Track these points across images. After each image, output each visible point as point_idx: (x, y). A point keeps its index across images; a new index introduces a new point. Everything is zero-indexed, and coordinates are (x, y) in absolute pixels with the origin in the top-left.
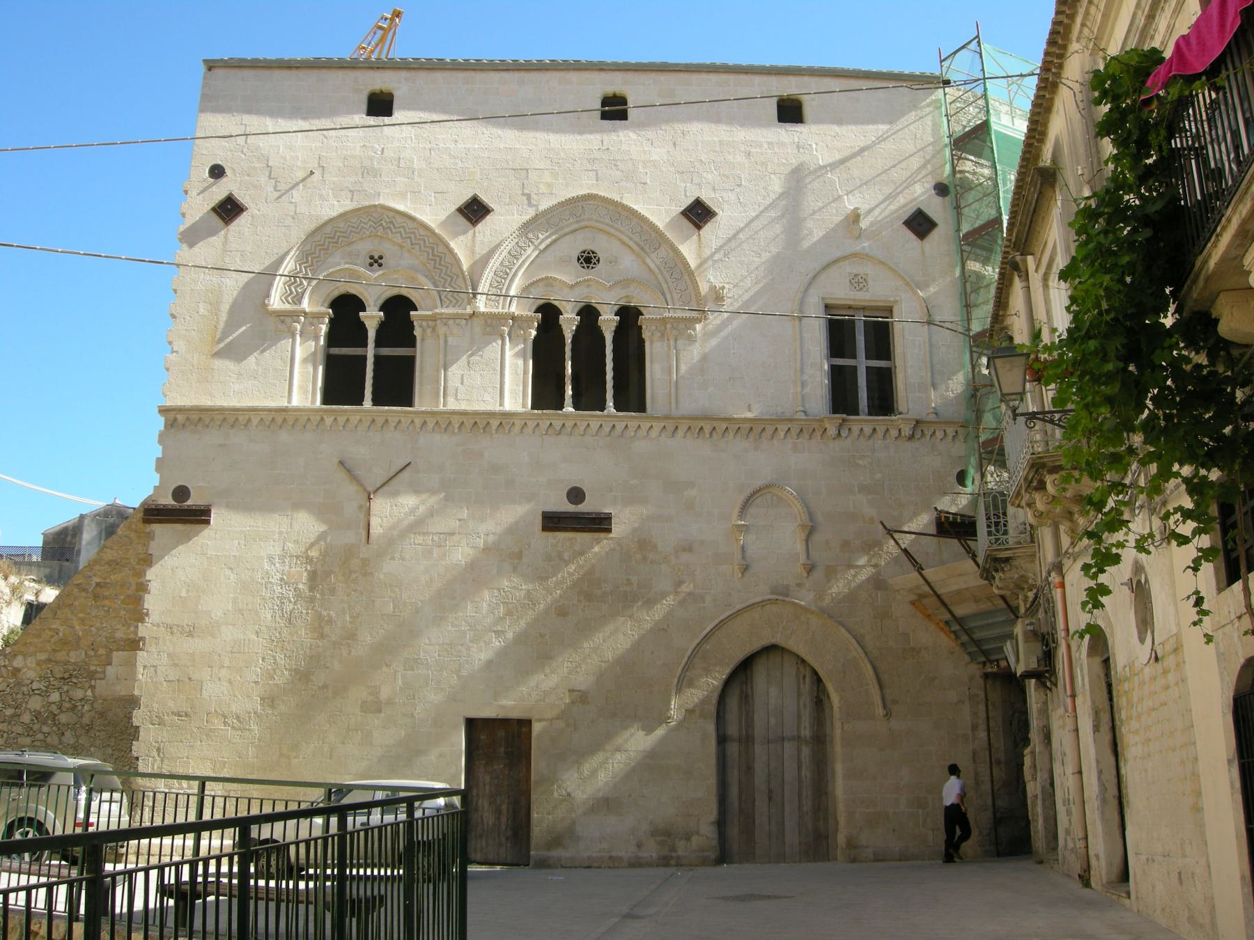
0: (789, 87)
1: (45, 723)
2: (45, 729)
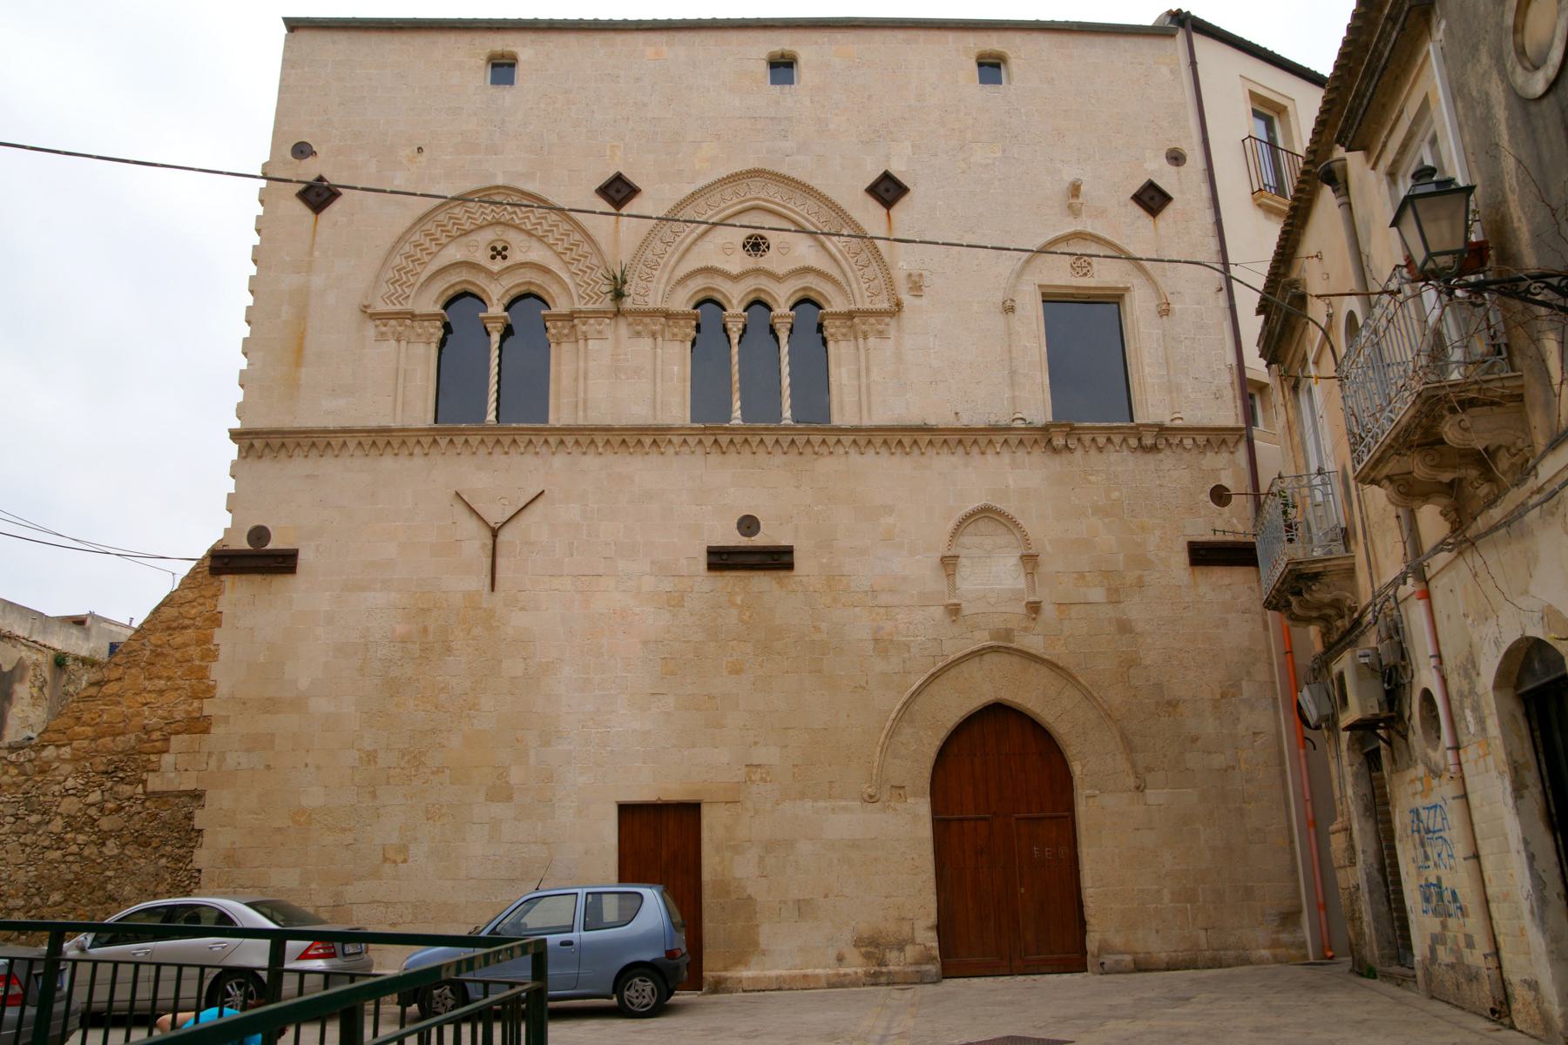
0: (992, 43)
1: (79, 831)
2: (81, 838)
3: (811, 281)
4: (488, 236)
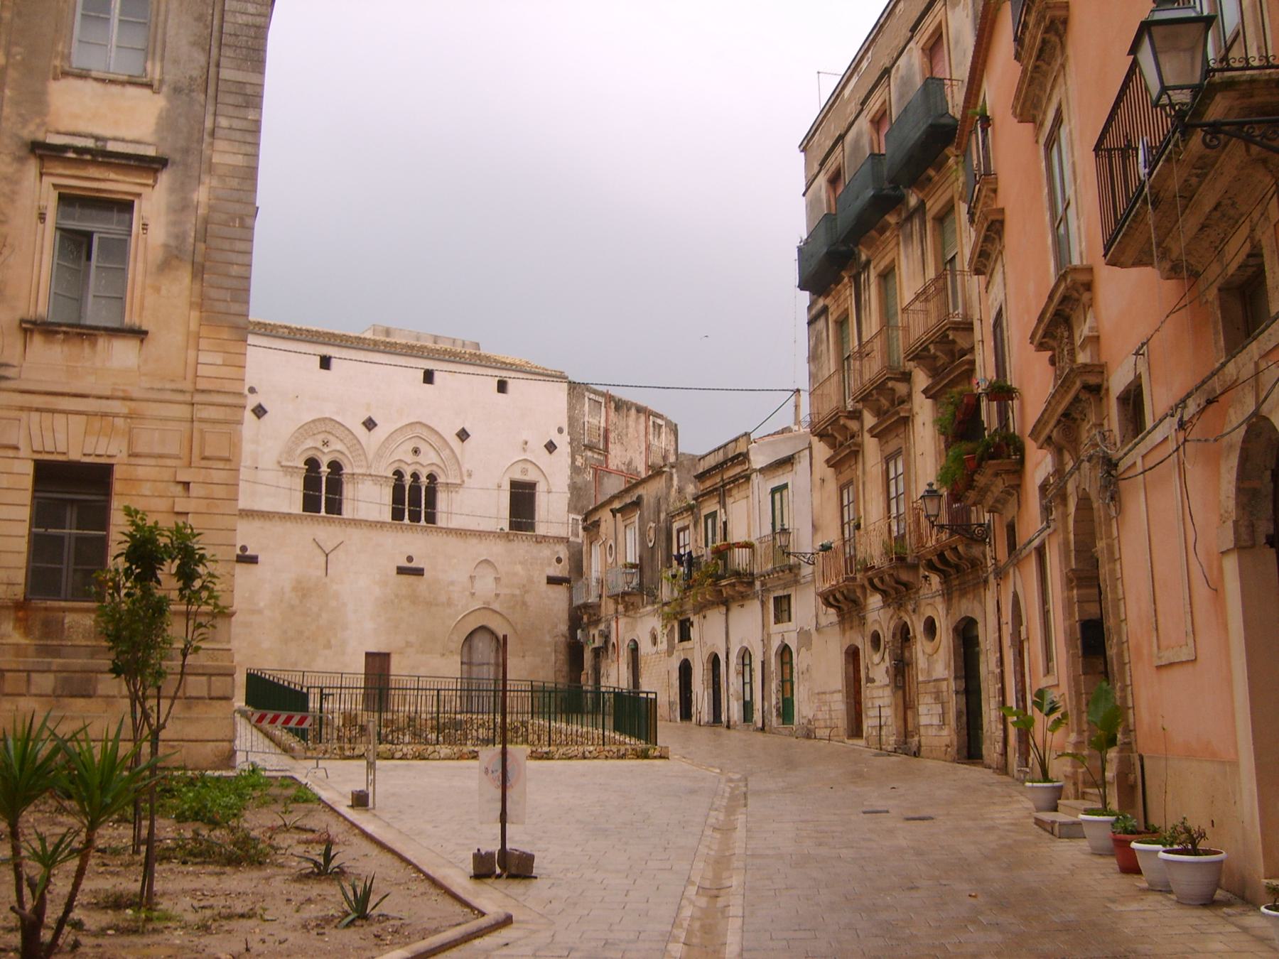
3: (434, 468)
4: (321, 437)
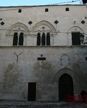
0: (67, 7)
